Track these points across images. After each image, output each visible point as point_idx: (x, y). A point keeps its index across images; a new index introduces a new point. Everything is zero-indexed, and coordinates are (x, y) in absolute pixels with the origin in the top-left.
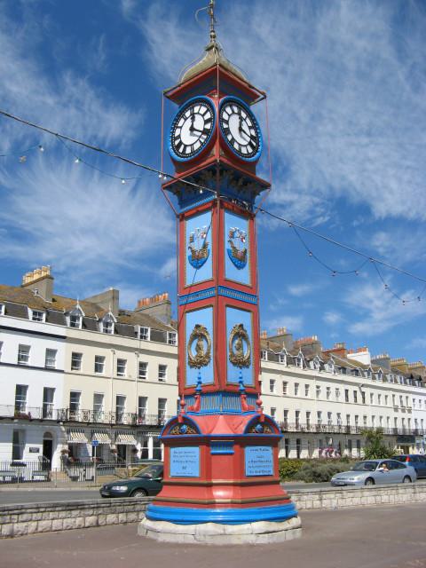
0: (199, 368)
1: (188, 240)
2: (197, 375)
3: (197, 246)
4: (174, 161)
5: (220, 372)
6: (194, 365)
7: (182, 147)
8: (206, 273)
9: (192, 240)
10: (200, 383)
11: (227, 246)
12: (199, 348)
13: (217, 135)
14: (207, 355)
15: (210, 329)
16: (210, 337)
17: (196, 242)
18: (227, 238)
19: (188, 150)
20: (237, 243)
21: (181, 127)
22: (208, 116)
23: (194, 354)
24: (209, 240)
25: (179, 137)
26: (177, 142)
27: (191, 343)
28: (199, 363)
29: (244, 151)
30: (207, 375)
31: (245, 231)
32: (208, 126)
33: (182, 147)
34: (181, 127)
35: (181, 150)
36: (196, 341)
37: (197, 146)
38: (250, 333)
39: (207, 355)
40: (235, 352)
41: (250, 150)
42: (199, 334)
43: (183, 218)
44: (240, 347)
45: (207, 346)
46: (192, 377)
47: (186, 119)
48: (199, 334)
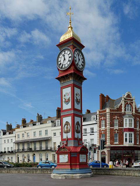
1: (63, 96)
3: (67, 97)
4: (58, 69)
5: (73, 135)
6: (65, 133)
7: (61, 65)
9: (65, 96)
10: (67, 138)
11: (75, 98)
12: (67, 128)
13: (73, 64)
15: (70, 123)
17: (66, 96)
18: (75, 96)
19: (63, 67)
20: (77, 97)
23: (65, 129)
26: (59, 63)
28: (67, 132)
29: (80, 67)
31: (80, 93)
33: (61, 65)
35: (61, 66)
36: (66, 126)
37: (66, 65)
38: (80, 124)
39: (70, 130)
40: (77, 129)
41: (82, 67)
42: (67, 123)
43: (62, 88)
44: (78, 128)
45: (70, 127)
46: (65, 136)
48: (67, 123)
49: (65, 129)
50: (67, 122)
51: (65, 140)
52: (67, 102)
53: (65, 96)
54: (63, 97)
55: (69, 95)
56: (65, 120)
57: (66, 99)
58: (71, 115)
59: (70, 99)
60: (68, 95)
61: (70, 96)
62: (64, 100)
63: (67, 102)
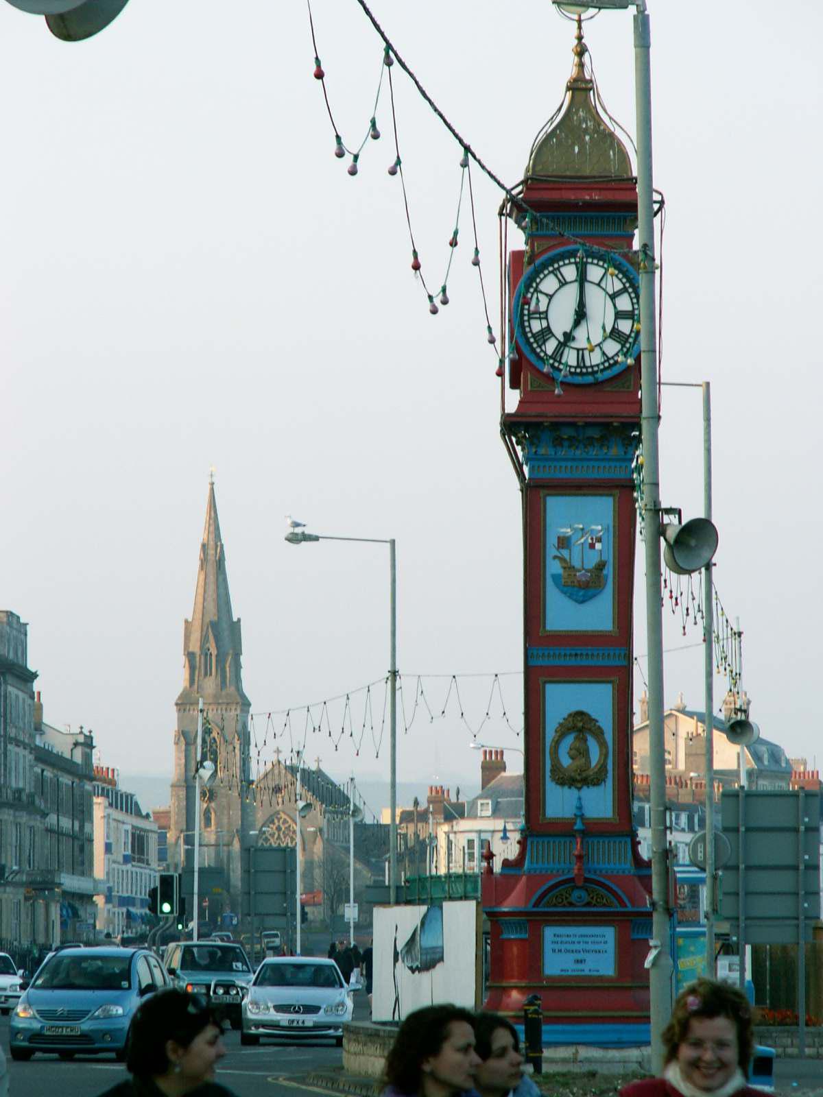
0: (579, 789)
1: (551, 541)
2: (575, 803)
3: (583, 560)
8: (596, 615)
12: (580, 752)
14: (603, 768)
15: (606, 721)
16: (609, 736)
21: (550, 297)
22: (624, 303)
23: (566, 761)
24: (609, 557)
25: (544, 315)
26: (536, 326)
27: (557, 743)
28: (579, 780)
30: (599, 803)
32: (625, 326)
34: (550, 297)
36: (569, 740)
37: (595, 358)
39: (603, 768)
42: (580, 724)
46: (560, 803)
47: (563, 283)
49: (566, 761)
50: (580, 714)
51: (562, 829)
52: (582, 587)
53: (564, 542)
54: (551, 550)
55: (598, 546)
56: (562, 700)
57: (576, 563)
58: (615, 679)
59: (609, 571)
60: (592, 546)
61: (605, 550)
62: (553, 567)
63: (585, 586)
